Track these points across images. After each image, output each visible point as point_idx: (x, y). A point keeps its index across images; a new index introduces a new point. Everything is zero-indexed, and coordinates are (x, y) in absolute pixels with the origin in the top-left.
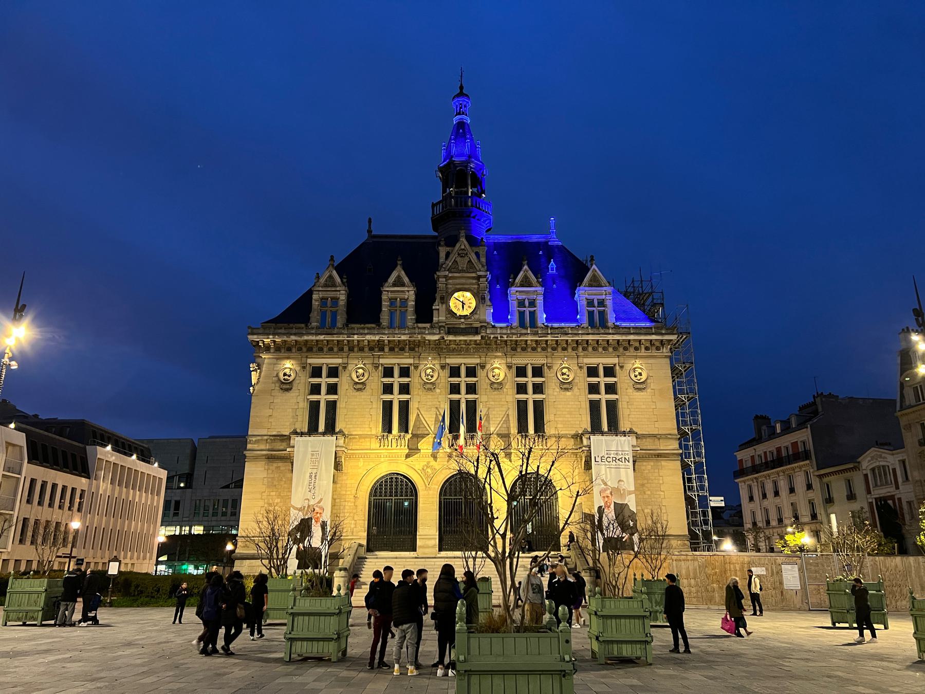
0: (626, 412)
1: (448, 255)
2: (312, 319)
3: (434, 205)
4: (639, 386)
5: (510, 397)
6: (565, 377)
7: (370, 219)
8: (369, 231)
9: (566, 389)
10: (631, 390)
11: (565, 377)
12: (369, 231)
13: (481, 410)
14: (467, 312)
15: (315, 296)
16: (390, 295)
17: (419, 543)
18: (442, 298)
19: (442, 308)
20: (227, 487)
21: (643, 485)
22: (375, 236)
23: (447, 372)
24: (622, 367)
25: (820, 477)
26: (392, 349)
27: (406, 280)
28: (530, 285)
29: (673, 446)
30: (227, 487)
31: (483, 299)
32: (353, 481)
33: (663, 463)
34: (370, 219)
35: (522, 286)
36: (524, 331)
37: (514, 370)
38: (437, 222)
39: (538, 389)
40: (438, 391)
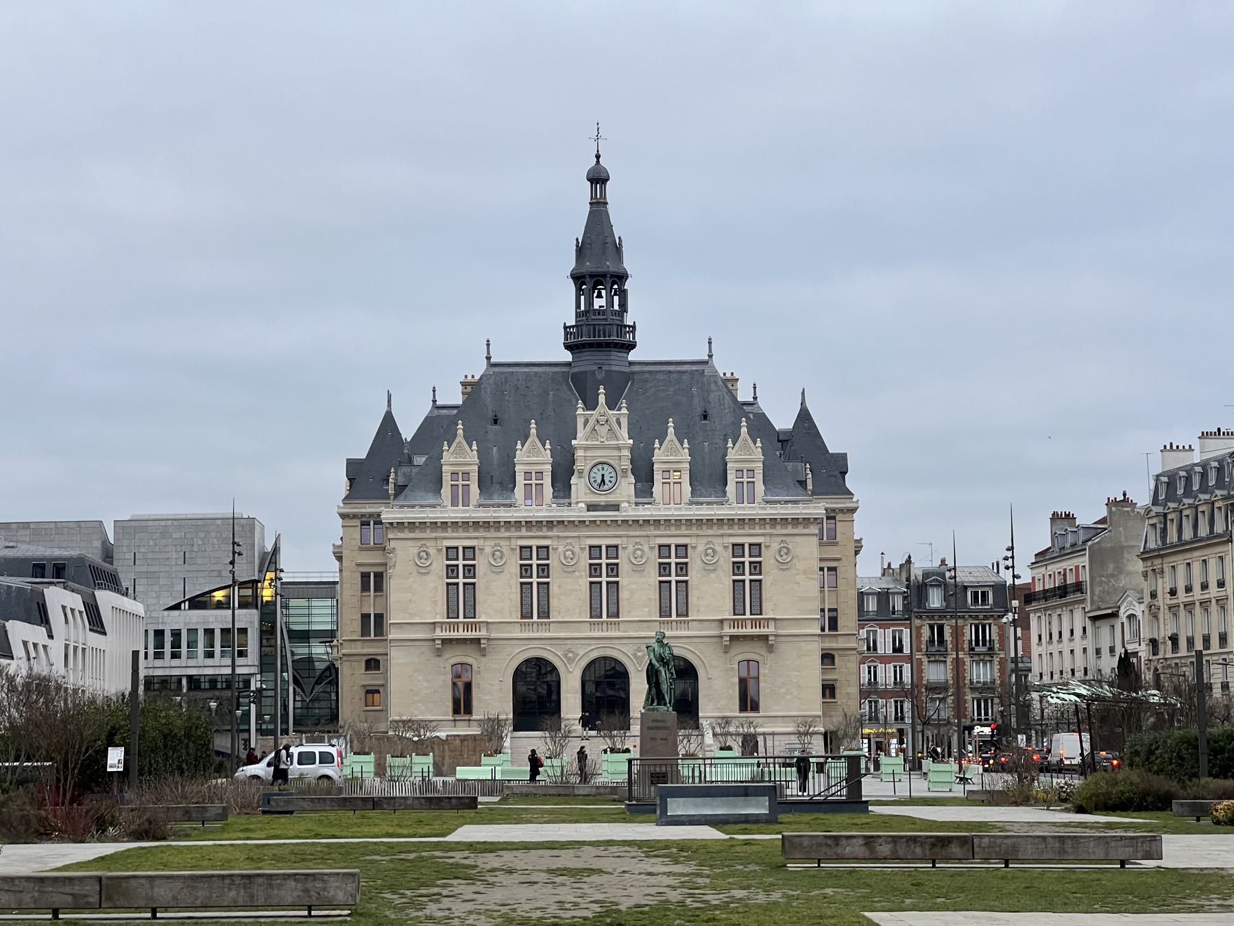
1: (586, 422)
3: (565, 328)
5: (654, 578)
8: (488, 358)
10: (776, 571)
12: (488, 358)
13: (624, 594)
16: (527, 468)
20: (177, 607)
22: (496, 365)
25: (1094, 619)
30: (177, 607)
38: (568, 347)
39: (683, 568)
40: (577, 574)
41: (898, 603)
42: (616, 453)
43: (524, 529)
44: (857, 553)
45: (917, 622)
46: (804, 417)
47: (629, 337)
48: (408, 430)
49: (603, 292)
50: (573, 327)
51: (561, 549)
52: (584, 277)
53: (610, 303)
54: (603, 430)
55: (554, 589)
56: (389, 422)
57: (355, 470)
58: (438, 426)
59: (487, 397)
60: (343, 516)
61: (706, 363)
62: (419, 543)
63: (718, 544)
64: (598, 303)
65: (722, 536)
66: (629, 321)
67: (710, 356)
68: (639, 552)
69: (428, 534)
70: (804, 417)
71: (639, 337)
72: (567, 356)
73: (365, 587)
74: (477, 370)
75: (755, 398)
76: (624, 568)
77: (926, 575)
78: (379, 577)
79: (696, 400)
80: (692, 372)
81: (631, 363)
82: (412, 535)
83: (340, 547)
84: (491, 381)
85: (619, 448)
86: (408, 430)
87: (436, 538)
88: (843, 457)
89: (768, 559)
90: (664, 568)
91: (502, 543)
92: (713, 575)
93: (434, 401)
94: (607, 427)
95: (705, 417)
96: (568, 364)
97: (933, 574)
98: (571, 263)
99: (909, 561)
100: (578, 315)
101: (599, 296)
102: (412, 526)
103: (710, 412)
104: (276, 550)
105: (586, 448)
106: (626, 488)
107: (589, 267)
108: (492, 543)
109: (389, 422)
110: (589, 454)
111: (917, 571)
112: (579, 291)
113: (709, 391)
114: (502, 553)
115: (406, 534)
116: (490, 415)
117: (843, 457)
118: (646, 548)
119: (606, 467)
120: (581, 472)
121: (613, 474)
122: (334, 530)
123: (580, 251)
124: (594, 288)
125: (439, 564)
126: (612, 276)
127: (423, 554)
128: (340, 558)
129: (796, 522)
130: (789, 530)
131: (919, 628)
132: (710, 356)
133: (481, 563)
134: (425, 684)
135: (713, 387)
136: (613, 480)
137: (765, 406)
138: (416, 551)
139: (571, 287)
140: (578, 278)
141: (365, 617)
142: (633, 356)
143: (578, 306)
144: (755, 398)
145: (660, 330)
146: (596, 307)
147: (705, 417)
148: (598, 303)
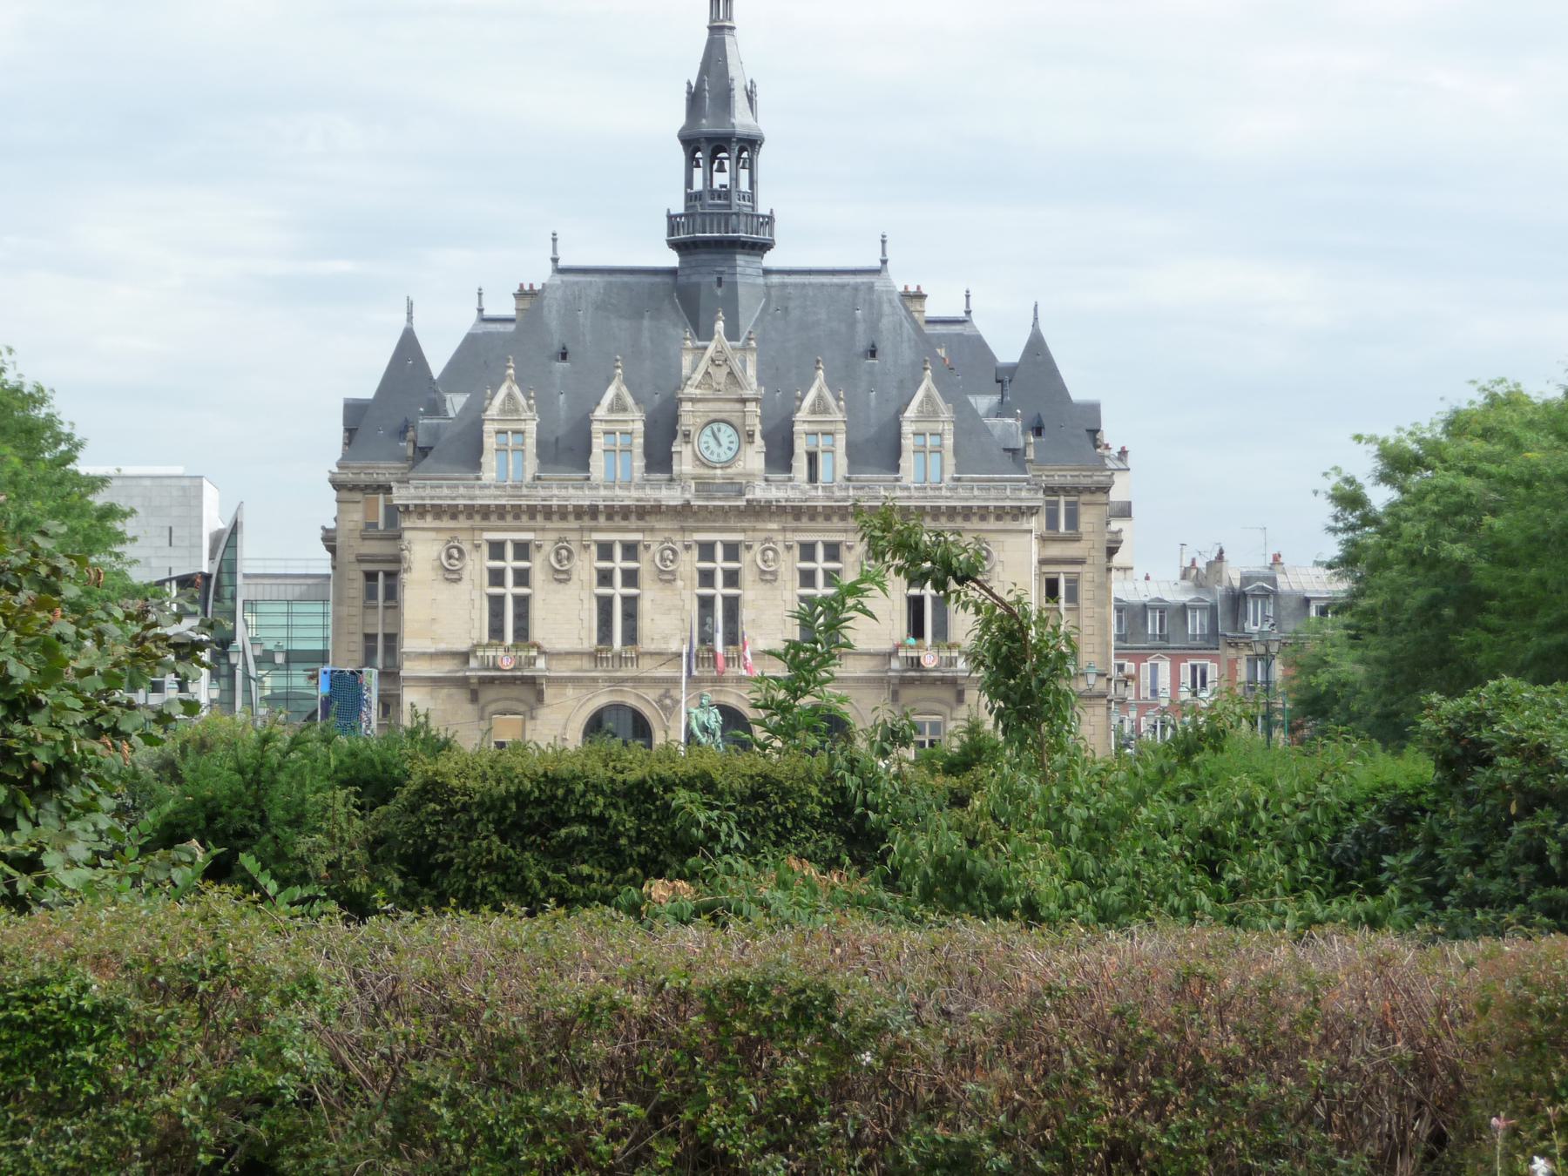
2: (485, 467)
3: (670, 217)
8: (555, 260)
12: (555, 260)
13: (746, 615)
14: (725, 455)
15: (489, 428)
19: (686, 451)
23: (695, 553)
26: (610, 517)
27: (629, 400)
28: (826, 411)
31: (751, 435)
36: (813, 493)
37: (797, 552)
40: (679, 583)
41: (1196, 624)
42: (738, 406)
43: (602, 519)
44: (1111, 552)
45: (1231, 652)
46: (1037, 347)
47: (763, 236)
48: (437, 359)
49: (727, 163)
50: (680, 216)
51: (655, 547)
52: (697, 140)
53: (735, 179)
54: (720, 375)
55: (645, 606)
56: (408, 348)
57: (357, 417)
58: (480, 356)
59: (552, 316)
60: (338, 486)
61: (876, 272)
62: (446, 536)
64: (721, 179)
66: (763, 209)
67: (884, 262)
68: (770, 554)
69: (463, 522)
70: (1037, 347)
71: (780, 233)
72: (672, 259)
73: (371, 594)
74: (539, 275)
75: (968, 313)
76: (748, 577)
77: (1246, 580)
78: (392, 576)
79: (861, 328)
80: (856, 288)
81: (767, 272)
82: (437, 524)
83: (334, 531)
84: (559, 294)
85: (744, 401)
86: (437, 359)
87: (473, 529)
88: (1093, 410)
91: (571, 536)
93: (481, 310)
94: (725, 370)
95: (873, 354)
96: (672, 272)
97: (1258, 579)
98: (679, 119)
99: (1220, 556)
100: (691, 198)
101: (721, 169)
102: (438, 512)
103: (879, 347)
104: (235, 529)
105: (692, 400)
106: (754, 459)
107: (707, 126)
108: (554, 536)
109: (408, 348)
110: (700, 406)
111: (1233, 574)
112: (692, 162)
113: (880, 316)
114: (569, 551)
115: (429, 521)
116: (557, 347)
117: (1093, 410)
118: (780, 548)
119: (723, 426)
120: (687, 435)
121: (734, 438)
122: (325, 508)
123: (695, 99)
124: (713, 158)
125: (478, 564)
126: (740, 140)
127: (455, 553)
128: (332, 549)
129: (1001, 513)
130: (992, 524)
131: (1232, 663)
132: (884, 262)
133: (537, 566)
135: (886, 308)
136: (735, 447)
137: (983, 325)
139: (679, 154)
140: (691, 143)
141: (370, 638)
142: (770, 260)
143: (689, 183)
144: (968, 313)
145: (811, 220)
146: (716, 186)
147: (873, 354)
148: (721, 179)
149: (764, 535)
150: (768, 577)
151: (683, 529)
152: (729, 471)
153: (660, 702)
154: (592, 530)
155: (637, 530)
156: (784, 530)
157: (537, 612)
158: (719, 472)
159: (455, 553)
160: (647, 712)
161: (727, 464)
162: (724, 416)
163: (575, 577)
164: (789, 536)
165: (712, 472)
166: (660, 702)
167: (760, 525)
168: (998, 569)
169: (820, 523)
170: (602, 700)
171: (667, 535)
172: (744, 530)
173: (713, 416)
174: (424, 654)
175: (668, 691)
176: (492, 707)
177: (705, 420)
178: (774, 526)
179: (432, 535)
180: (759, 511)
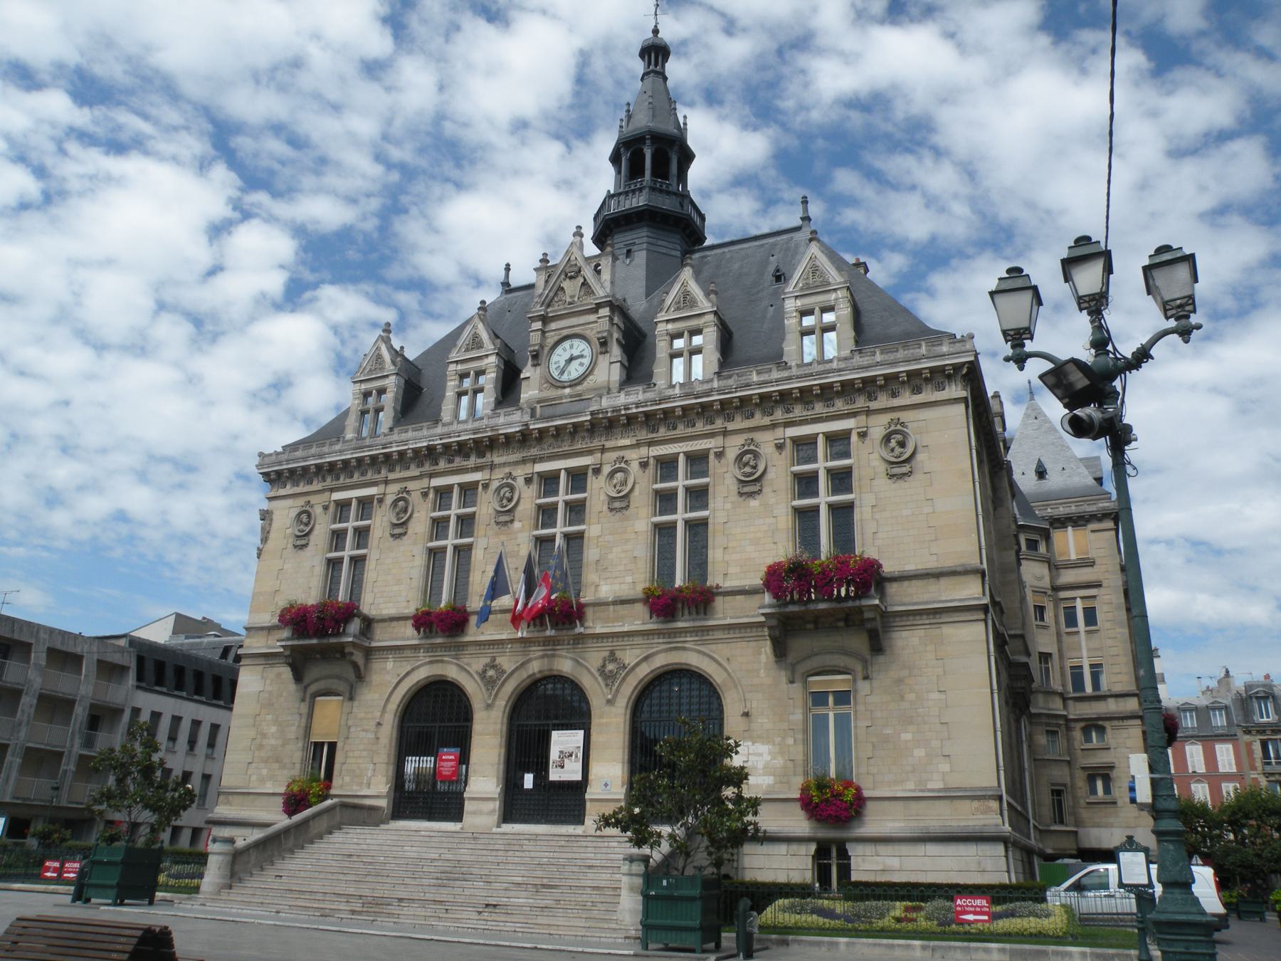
0: (870, 528)
4: (897, 470)
5: (642, 519)
6: (748, 469)
7: (508, 265)
9: (751, 495)
10: (883, 483)
11: (748, 469)
17: (468, 806)
18: (536, 356)
21: (900, 681)
23: (534, 486)
24: (863, 435)
29: (971, 591)
32: (377, 696)
33: (946, 630)
34: (508, 265)
35: (678, 309)
39: (699, 496)
40: (517, 525)
42: (592, 317)
62: (300, 502)
63: (766, 441)
65: (774, 426)
89: (867, 459)
90: (665, 500)
92: (754, 503)
106: (610, 370)
118: (635, 467)
127: (304, 517)
130: (906, 398)
134: (273, 729)
138: (294, 513)
149: (612, 456)
150: (617, 505)
151: (524, 461)
152: (579, 388)
153: (482, 675)
154: (431, 476)
155: (477, 469)
156: (638, 445)
157: (371, 572)
158: (567, 391)
159: (305, 518)
160: (471, 687)
161: (574, 383)
162: (576, 330)
163: (410, 532)
164: (644, 451)
165: (560, 392)
166: (482, 675)
167: (608, 444)
168: (920, 457)
169: (681, 430)
170: (422, 674)
171: (507, 470)
172: (590, 452)
173: (565, 332)
174: (262, 628)
175: (494, 659)
176: (313, 688)
177: (556, 338)
178: (627, 442)
179: (289, 502)
180: (607, 424)
